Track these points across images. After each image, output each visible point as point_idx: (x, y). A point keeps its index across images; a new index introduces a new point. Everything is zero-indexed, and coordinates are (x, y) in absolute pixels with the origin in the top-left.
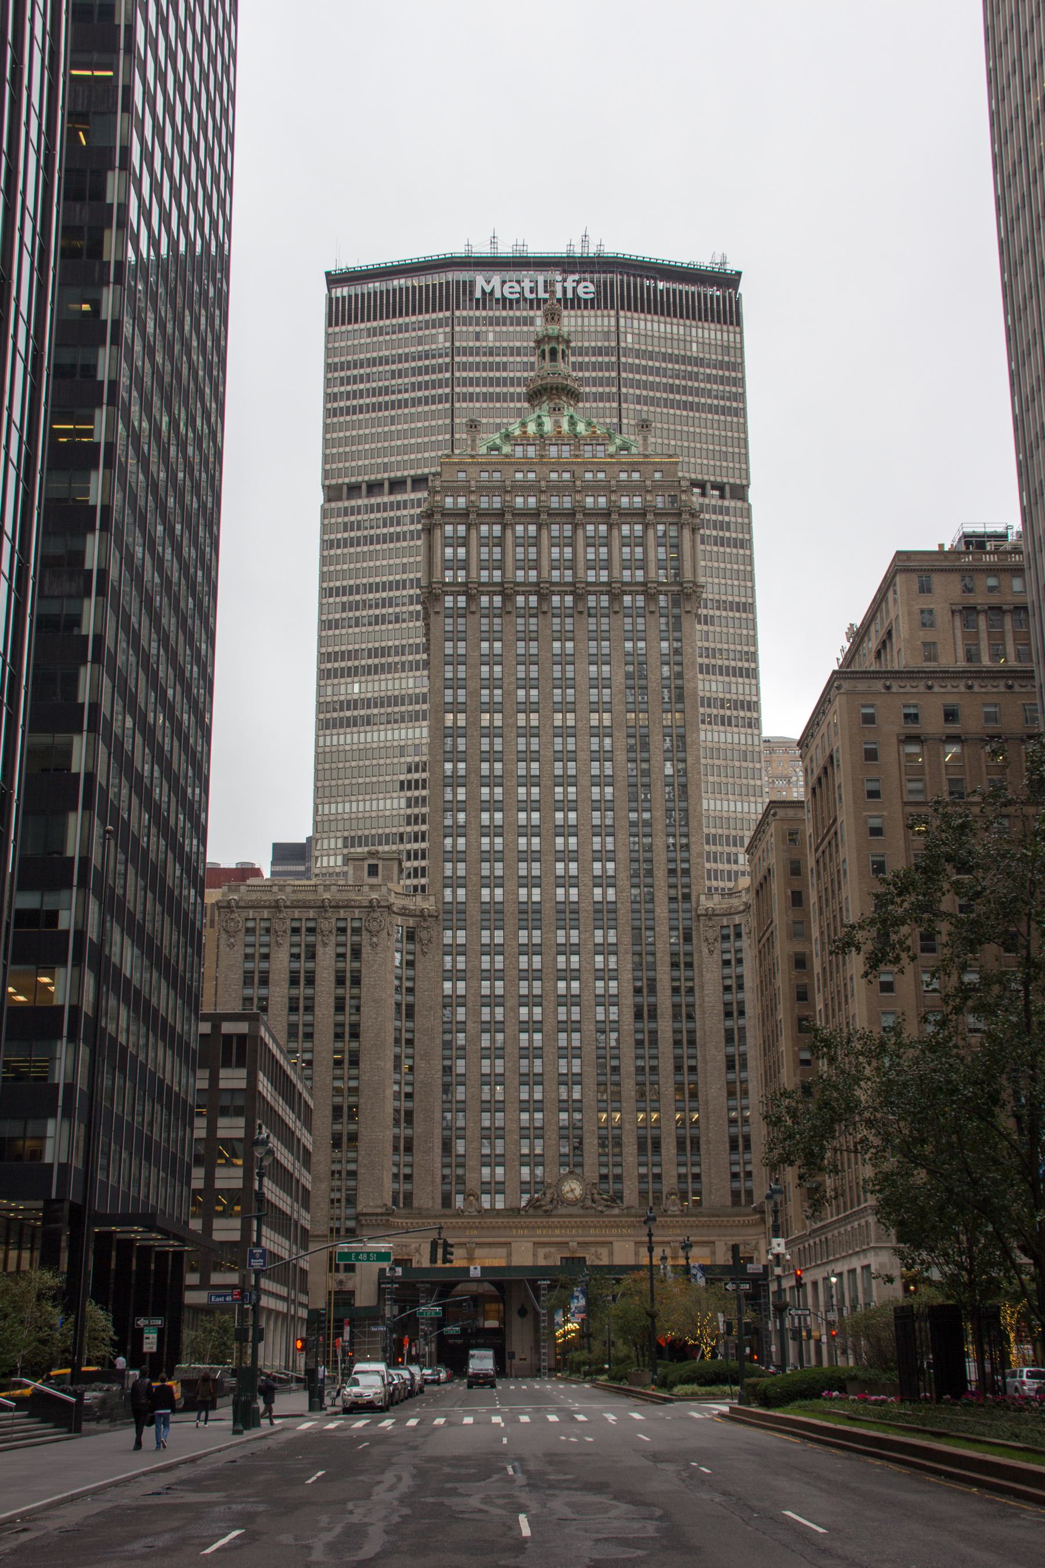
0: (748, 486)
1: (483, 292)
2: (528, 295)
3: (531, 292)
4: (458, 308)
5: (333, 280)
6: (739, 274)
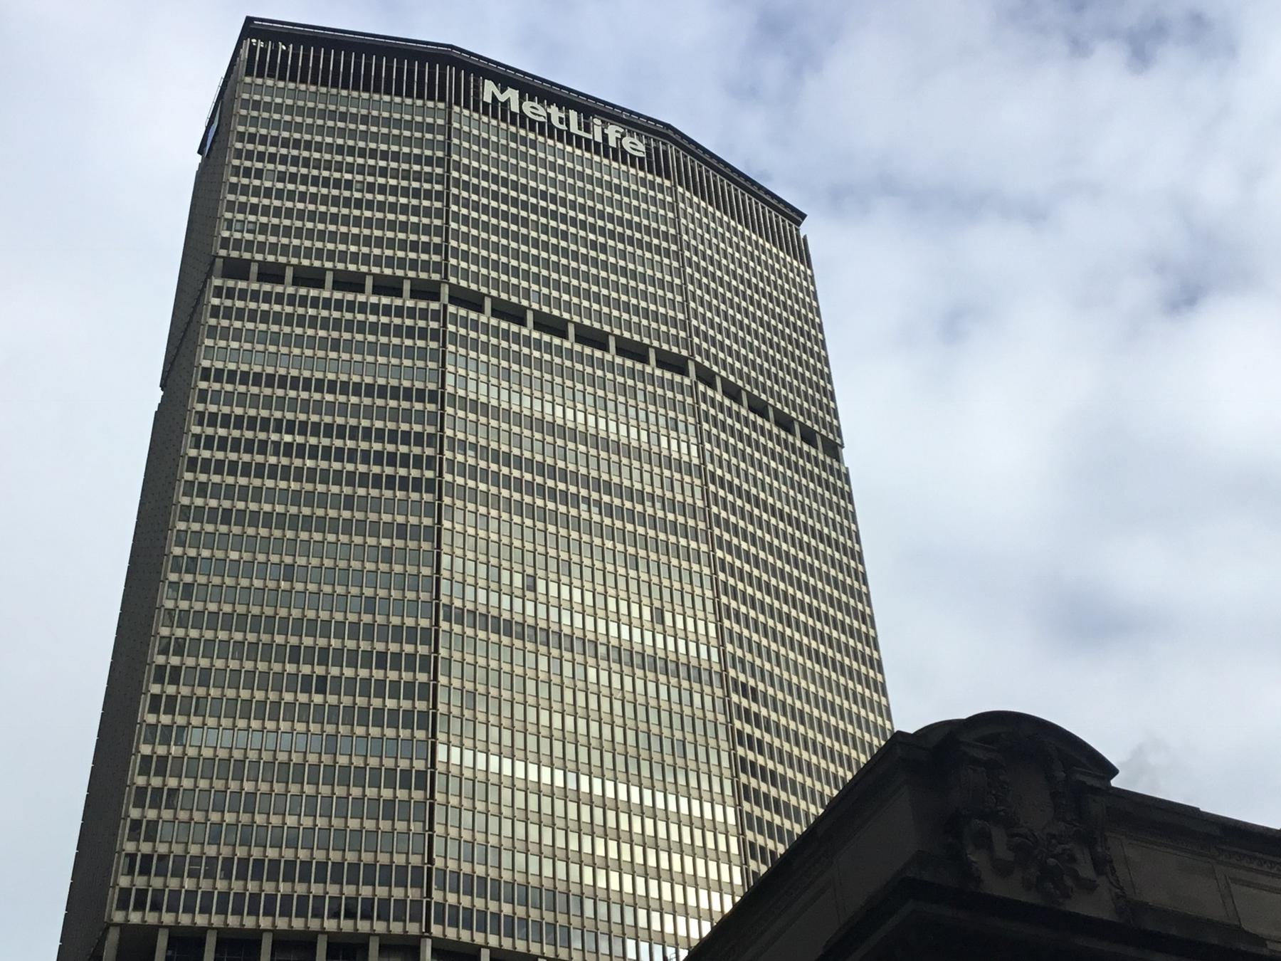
0: (842, 446)
1: (494, 98)
2: (555, 122)
3: (561, 122)
4: (458, 103)
5: (251, 28)
6: (803, 216)
